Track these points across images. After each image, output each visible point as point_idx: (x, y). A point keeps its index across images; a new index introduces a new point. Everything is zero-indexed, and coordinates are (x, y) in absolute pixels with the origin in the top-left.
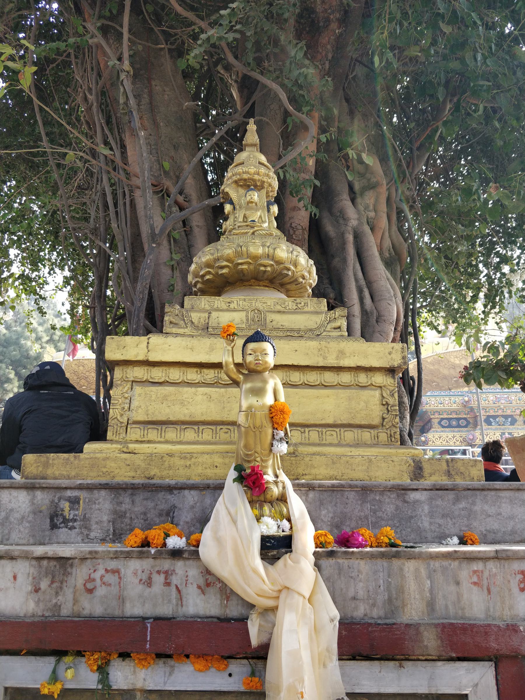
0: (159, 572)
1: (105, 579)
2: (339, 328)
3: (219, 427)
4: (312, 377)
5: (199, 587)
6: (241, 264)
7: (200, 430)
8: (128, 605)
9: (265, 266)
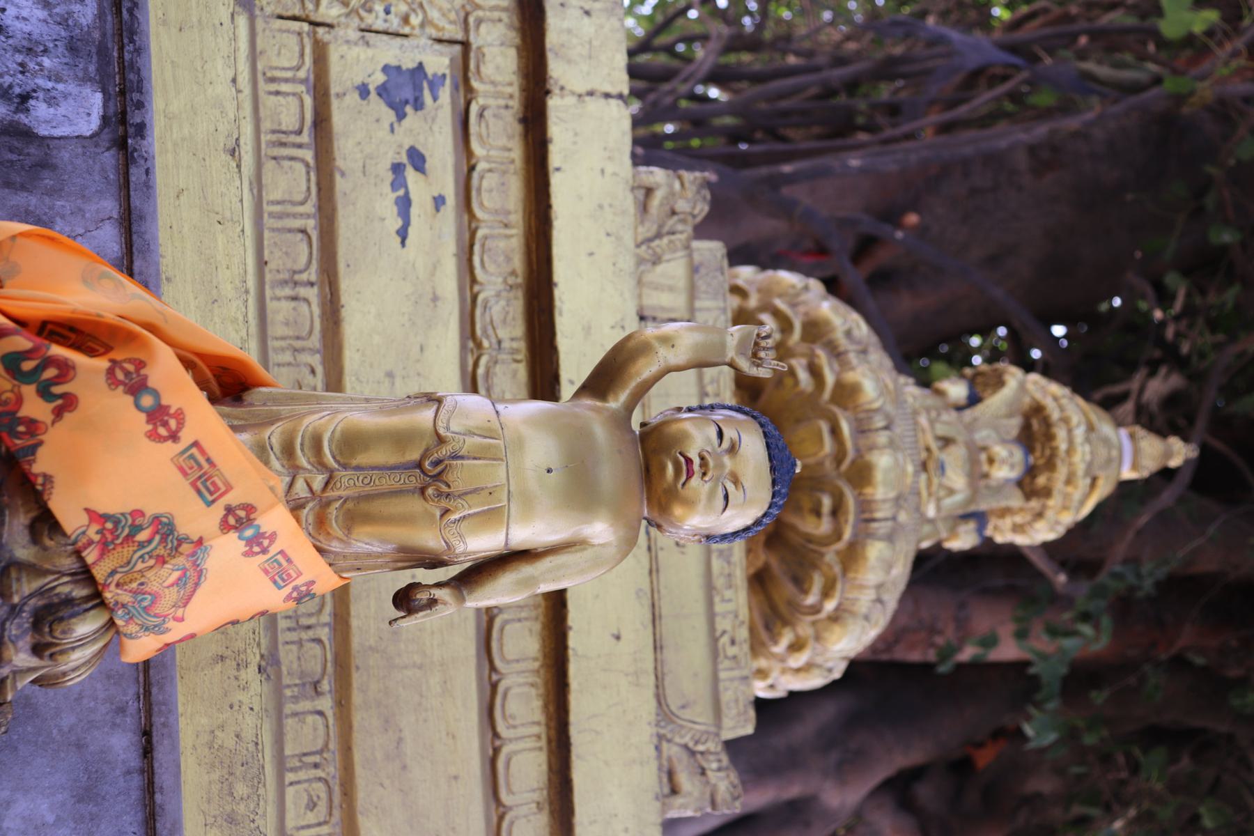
2: (674, 791)
3: (316, 360)
4: (524, 707)
6: (835, 431)
7: (303, 292)
9: (836, 512)
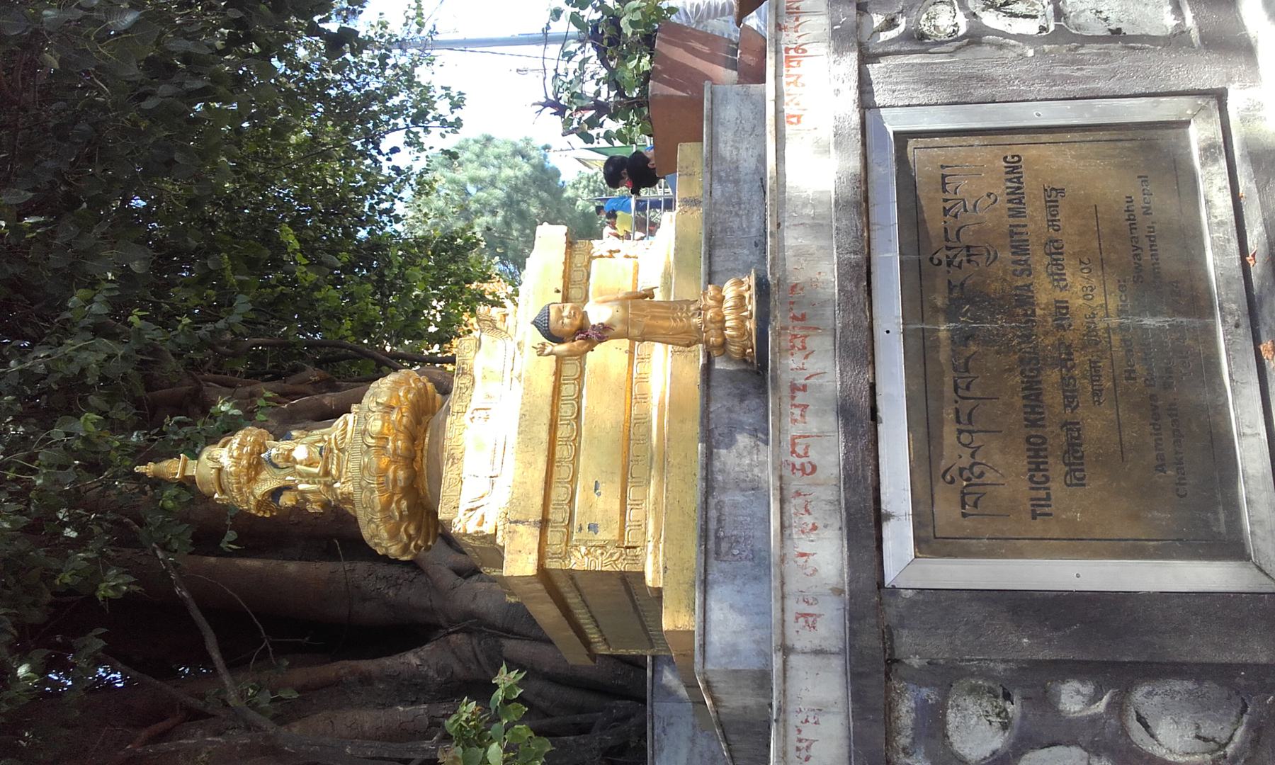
0: (793, 398)
1: (802, 453)
5: (806, 357)
8: (826, 428)
